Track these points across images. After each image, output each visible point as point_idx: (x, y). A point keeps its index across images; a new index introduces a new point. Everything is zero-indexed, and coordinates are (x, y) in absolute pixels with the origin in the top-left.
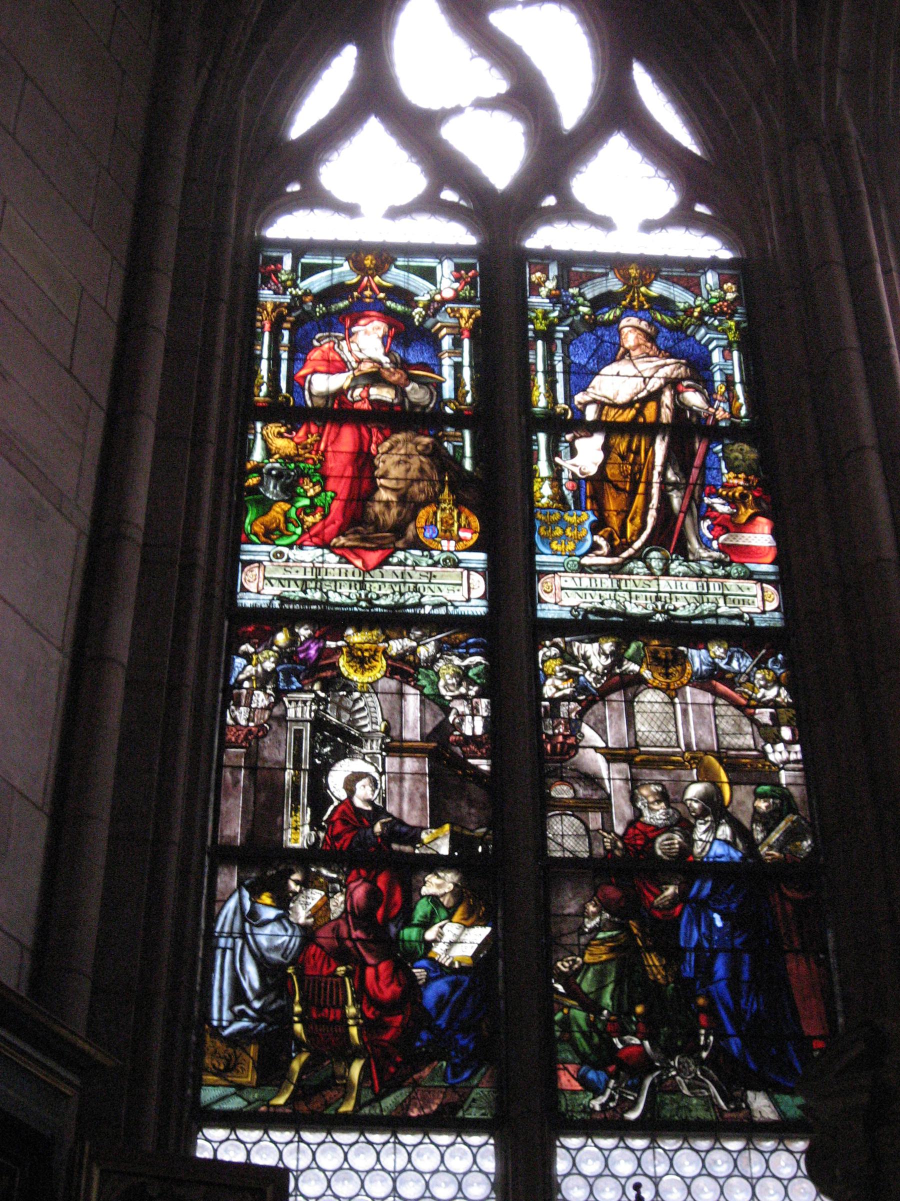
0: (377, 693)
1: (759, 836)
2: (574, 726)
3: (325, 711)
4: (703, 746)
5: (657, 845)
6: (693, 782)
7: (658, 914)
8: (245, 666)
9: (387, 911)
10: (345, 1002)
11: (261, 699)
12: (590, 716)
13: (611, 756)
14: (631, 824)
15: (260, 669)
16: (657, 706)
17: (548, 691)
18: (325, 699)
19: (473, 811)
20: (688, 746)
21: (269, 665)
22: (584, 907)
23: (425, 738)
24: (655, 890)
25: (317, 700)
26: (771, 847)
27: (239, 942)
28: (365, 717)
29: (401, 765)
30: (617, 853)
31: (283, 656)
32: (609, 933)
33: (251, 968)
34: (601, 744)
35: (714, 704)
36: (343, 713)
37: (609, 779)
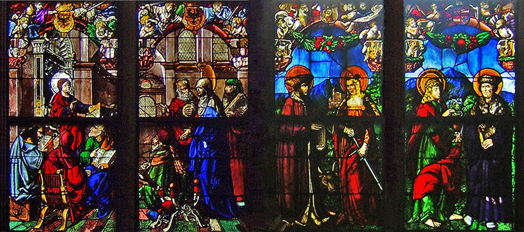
0: (70, 38)
1: (225, 105)
2: (152, 51)
3: (48, 48)
4: (206, 60)
5: (183, 110)
6: (201, 79)
7: (182, 143)
8: (15, 26)
9: (76, 145)
10: (61, 185)
11: (22, 43)
12: (159, 47)
13: (167, 67)
14: (173, 100)
15: (21, 28)
16: (188, 39)
17: (142, 34)
18: (48, 42)
19: (109, 96)
20: (200, 59)
21: (25, 25)
22: (152, 140)
23: (91, 60)
24: (182, 132)
25: (46, 43)
26: (230, 110)
27: (20, 160)
28: (65, 50)
29: (80, 74)
30: (167, 114)
31: (32, 20)
32: (161, 152)
33: (25, 172)
34: (163, 60)
35: (213, 37)
36: (56, 49)
37: (166, 78)
